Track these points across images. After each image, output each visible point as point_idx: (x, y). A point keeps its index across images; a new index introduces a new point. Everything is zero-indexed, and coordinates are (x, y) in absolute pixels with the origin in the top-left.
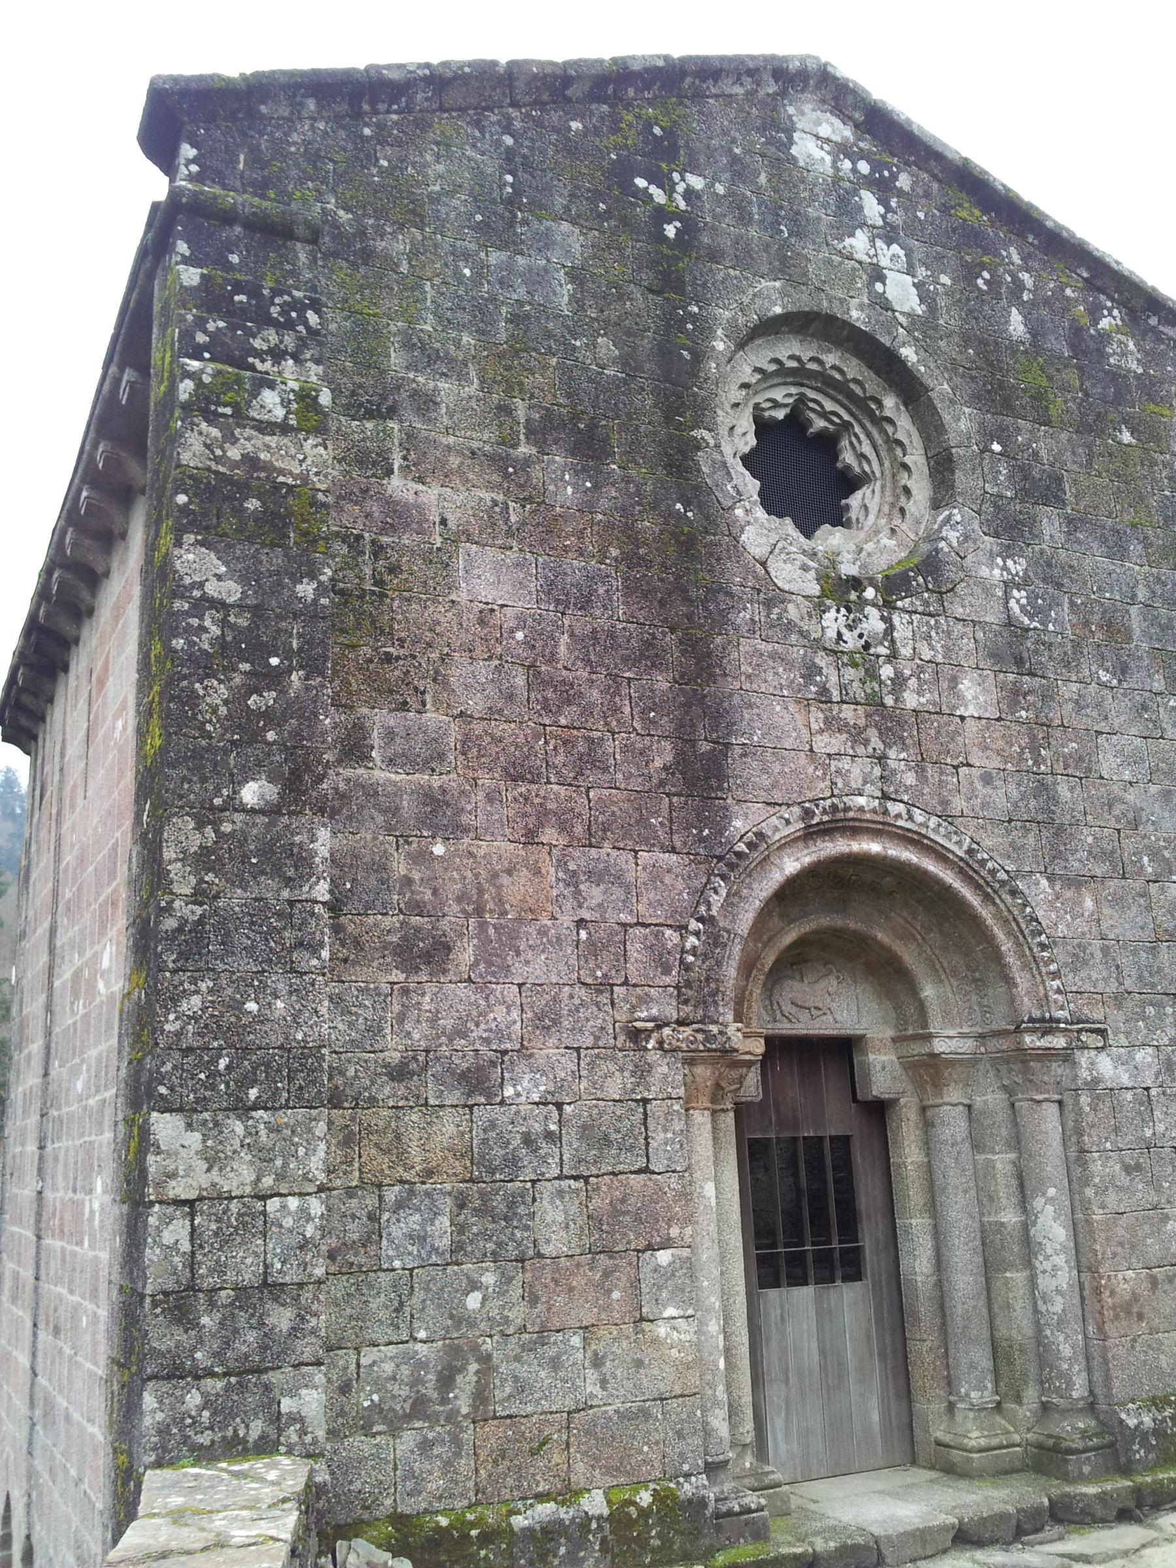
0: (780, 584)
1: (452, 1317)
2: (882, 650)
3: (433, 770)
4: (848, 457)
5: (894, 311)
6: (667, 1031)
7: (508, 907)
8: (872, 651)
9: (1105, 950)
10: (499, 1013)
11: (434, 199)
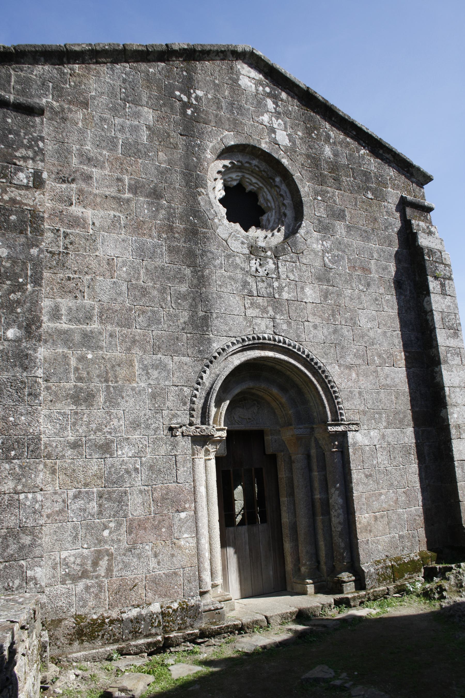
0: (233, 249)
1: (97, 539)
2: (274, 276)
3: (88, 324)
5: (279, 145)
6: (184, 428)
7: (118, 379)
8: (270, 276)
9: (360, 393)
10: (115, 422)
11: (93, 98)
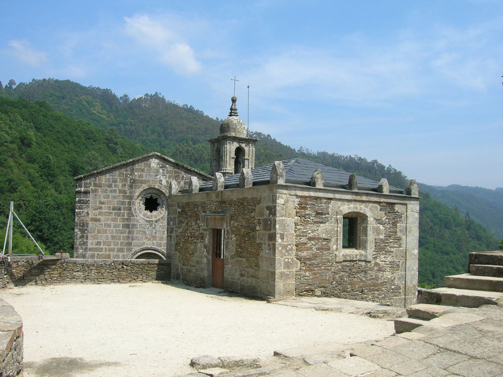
4: (158, 202)
